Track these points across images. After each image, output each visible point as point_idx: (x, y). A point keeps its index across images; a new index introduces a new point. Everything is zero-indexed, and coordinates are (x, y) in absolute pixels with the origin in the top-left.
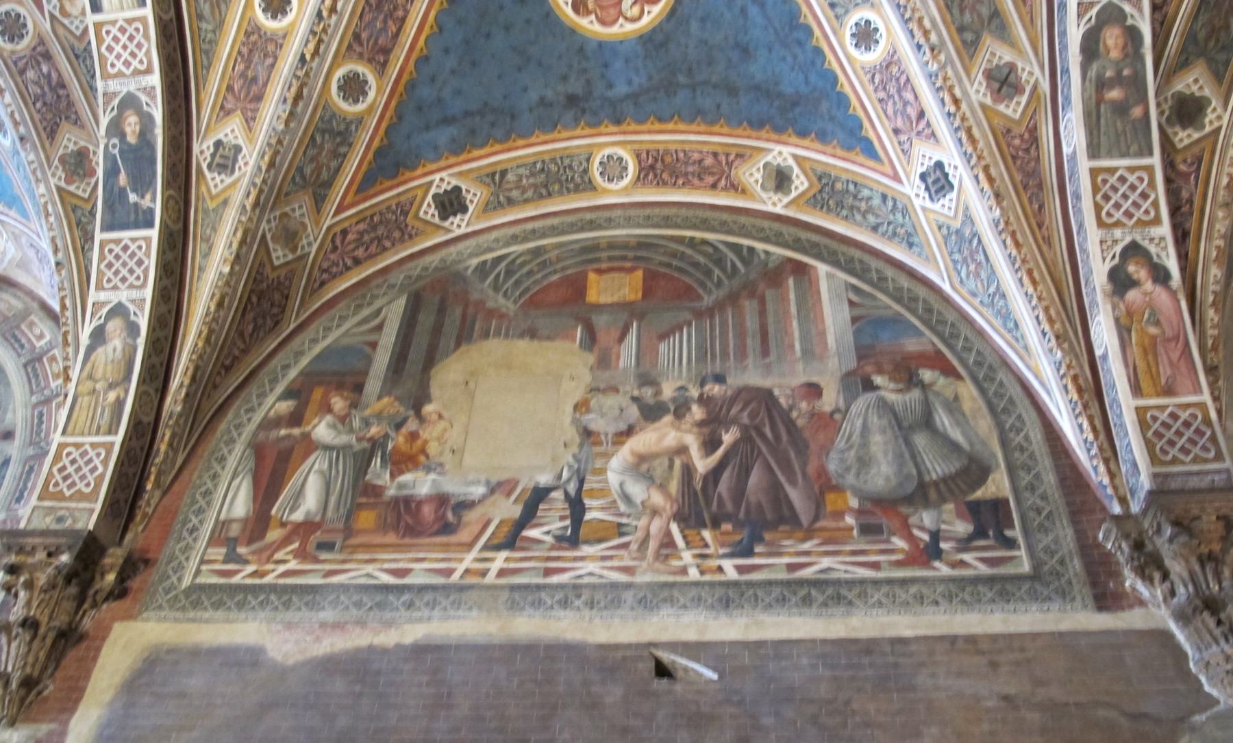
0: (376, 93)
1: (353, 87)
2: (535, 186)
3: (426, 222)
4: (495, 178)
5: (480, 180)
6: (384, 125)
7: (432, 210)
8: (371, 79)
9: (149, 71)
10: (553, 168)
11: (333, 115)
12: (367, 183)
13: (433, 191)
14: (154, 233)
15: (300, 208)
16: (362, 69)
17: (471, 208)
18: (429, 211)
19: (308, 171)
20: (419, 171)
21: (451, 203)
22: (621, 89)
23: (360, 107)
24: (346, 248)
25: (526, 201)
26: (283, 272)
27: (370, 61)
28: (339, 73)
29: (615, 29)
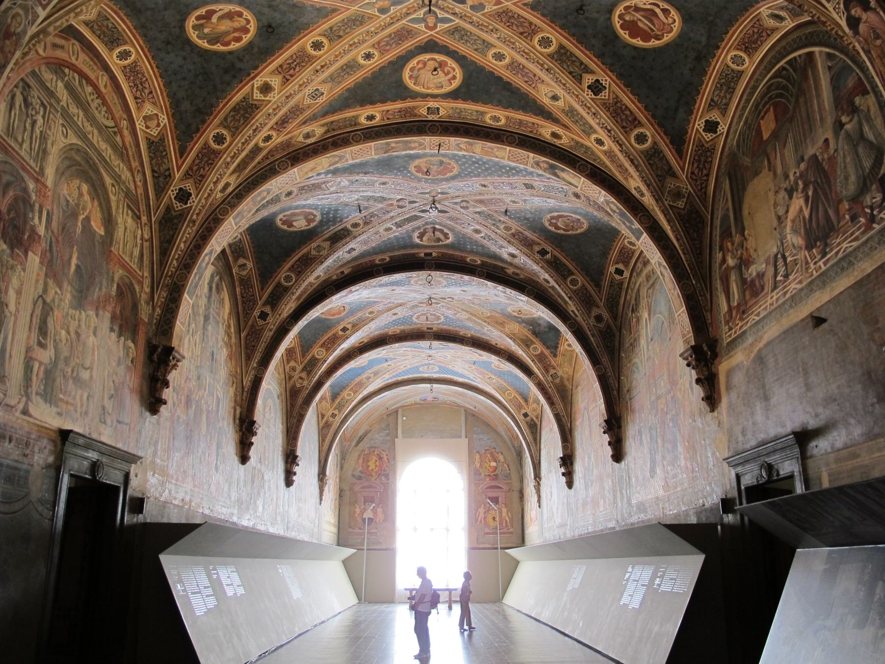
0: (648, 131)
1: (641, 139)
2: (725, 92)
3: (712, 140)
4: (712, 105)
5: (709, 110)
6: (662, 135)
7: (709, 135)
8: (641, 130)
9: (600, 192)
10: (723, 81)
11: (647, 151)
12: (680, 153)
13: (701, 130)
14: (645, 234)
15: (671, 184)
16: (636, 132)
17: (719, 120)
18: (708, 136)
19: (660, 173)
20: (690, 131)
21: (711, 127)
22: (704, 40)
23: (650, 140)
24: (699, 178)
25: (730, 99)
26: (688, 206)
27: (635, 127)
28: (633, 140)
29: (675, 29)
